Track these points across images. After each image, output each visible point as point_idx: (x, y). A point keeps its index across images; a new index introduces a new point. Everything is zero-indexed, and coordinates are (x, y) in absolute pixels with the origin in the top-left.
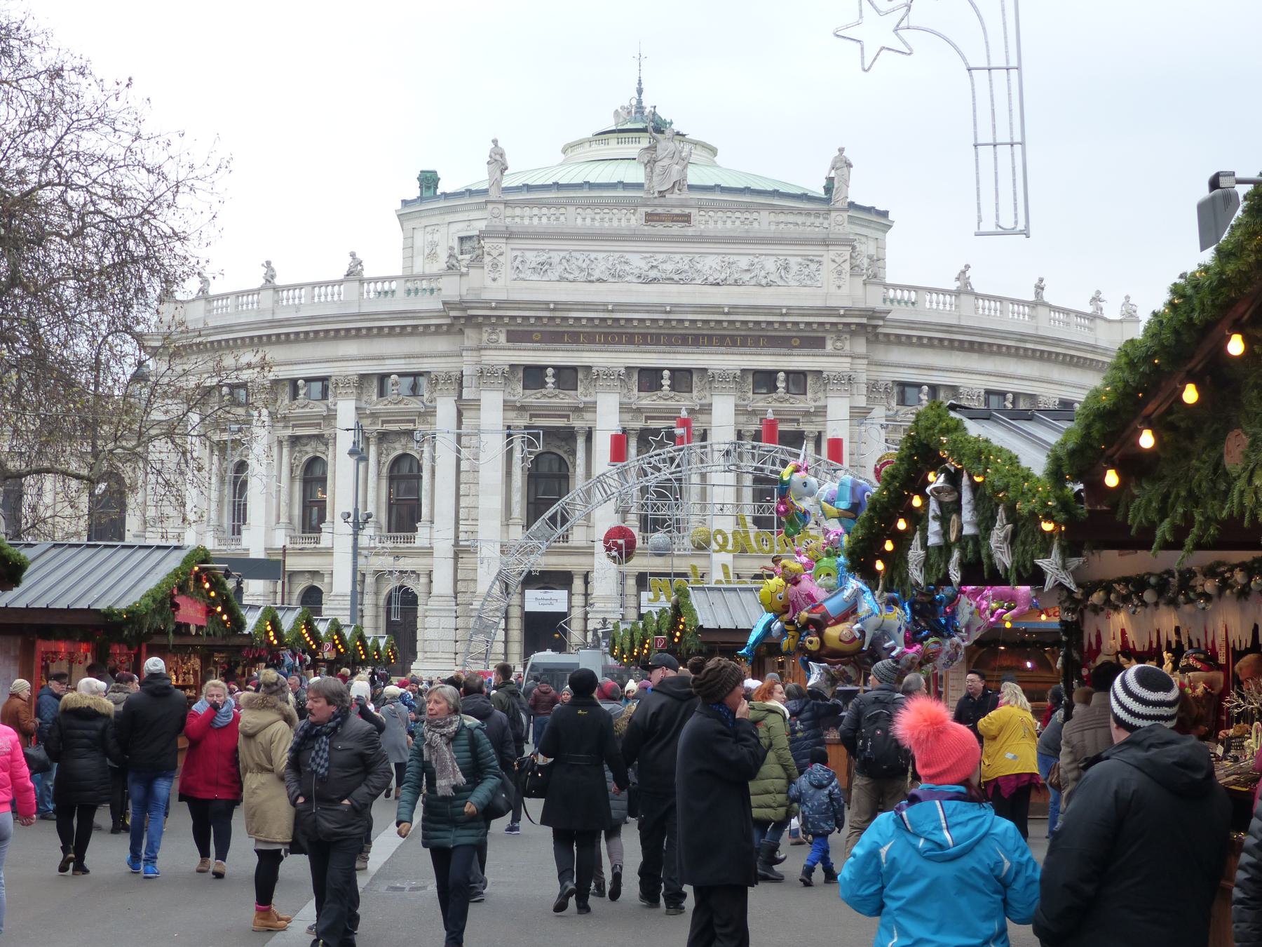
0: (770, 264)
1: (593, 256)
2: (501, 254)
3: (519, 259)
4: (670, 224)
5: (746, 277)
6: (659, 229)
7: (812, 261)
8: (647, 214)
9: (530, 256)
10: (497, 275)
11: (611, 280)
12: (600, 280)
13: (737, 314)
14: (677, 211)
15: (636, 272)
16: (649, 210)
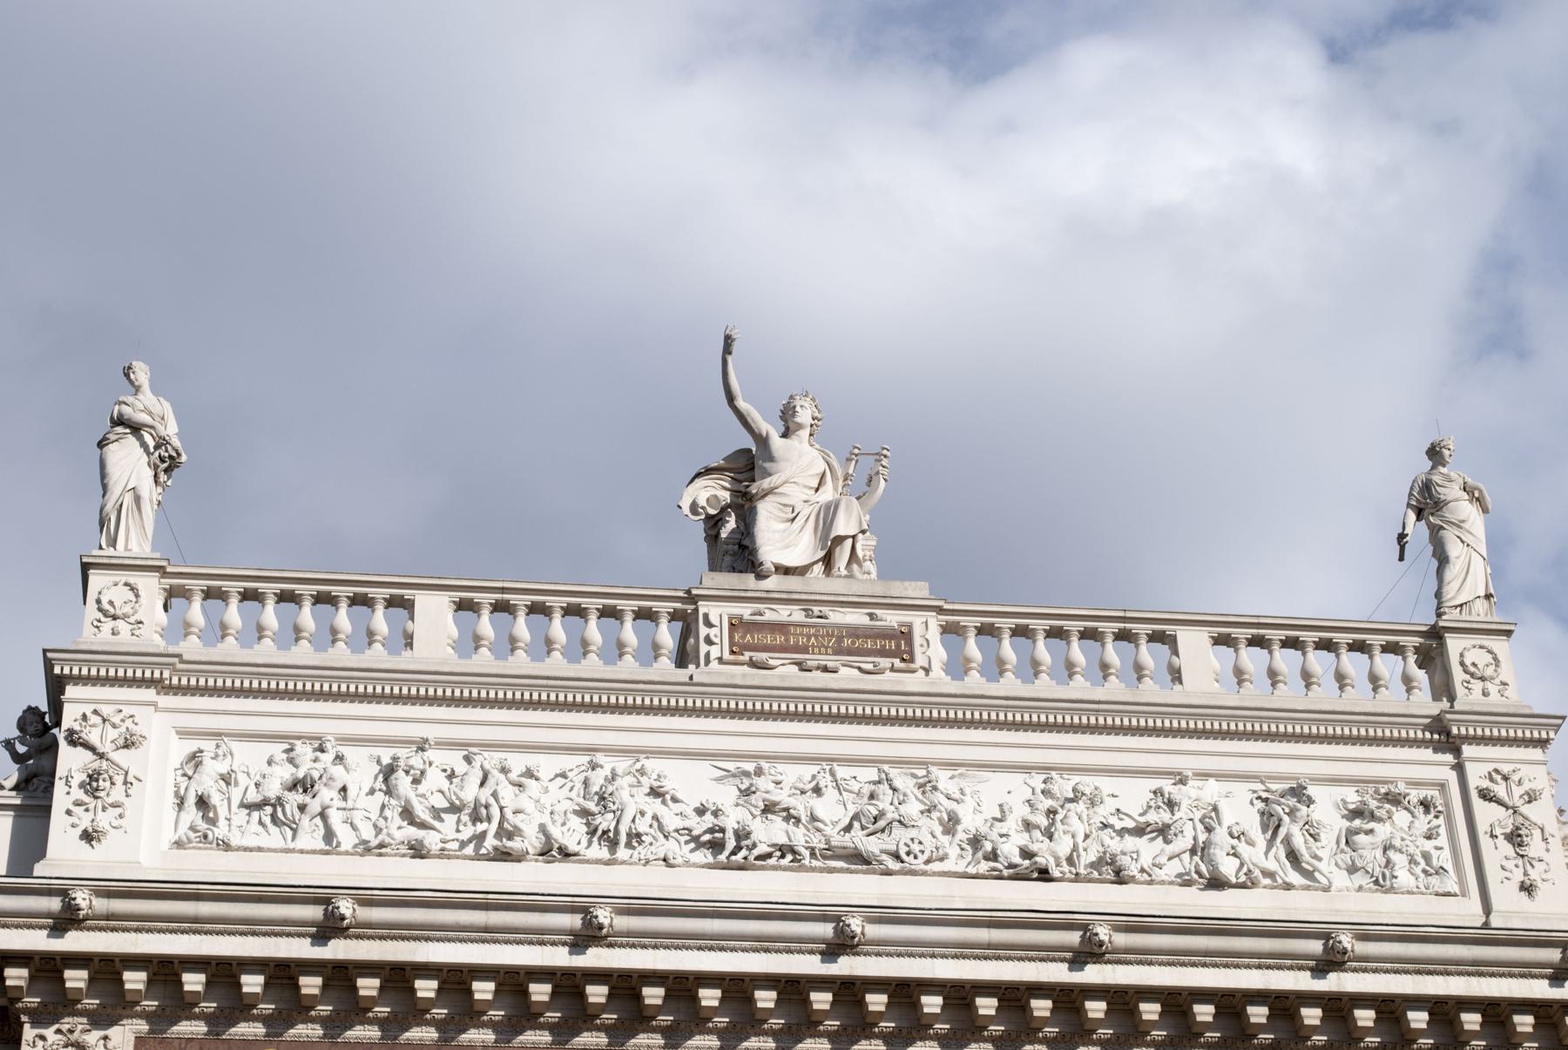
0: (1240, 810)
1: (517, 763)
2: (128, 745)
3: (212, 768)
4: (831, 661)
5: (1148, 850)
6: (784, 671)
7: (1394, 799)
8: (736, 625)
9: (249, 757)
10: (104, 820)
11: (599, 851)
12: (553, 852)
13: (1144, 957)
14: (857, 618)
15: (700, 825)
16: (745, 611)
